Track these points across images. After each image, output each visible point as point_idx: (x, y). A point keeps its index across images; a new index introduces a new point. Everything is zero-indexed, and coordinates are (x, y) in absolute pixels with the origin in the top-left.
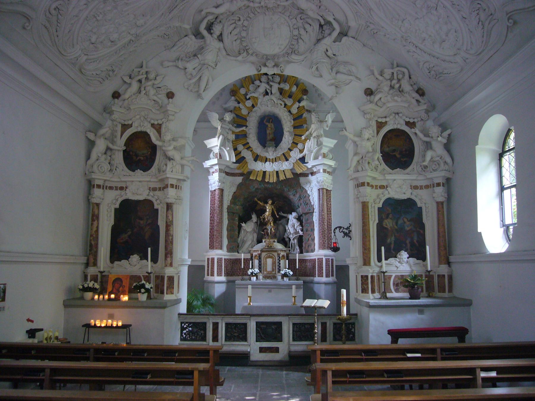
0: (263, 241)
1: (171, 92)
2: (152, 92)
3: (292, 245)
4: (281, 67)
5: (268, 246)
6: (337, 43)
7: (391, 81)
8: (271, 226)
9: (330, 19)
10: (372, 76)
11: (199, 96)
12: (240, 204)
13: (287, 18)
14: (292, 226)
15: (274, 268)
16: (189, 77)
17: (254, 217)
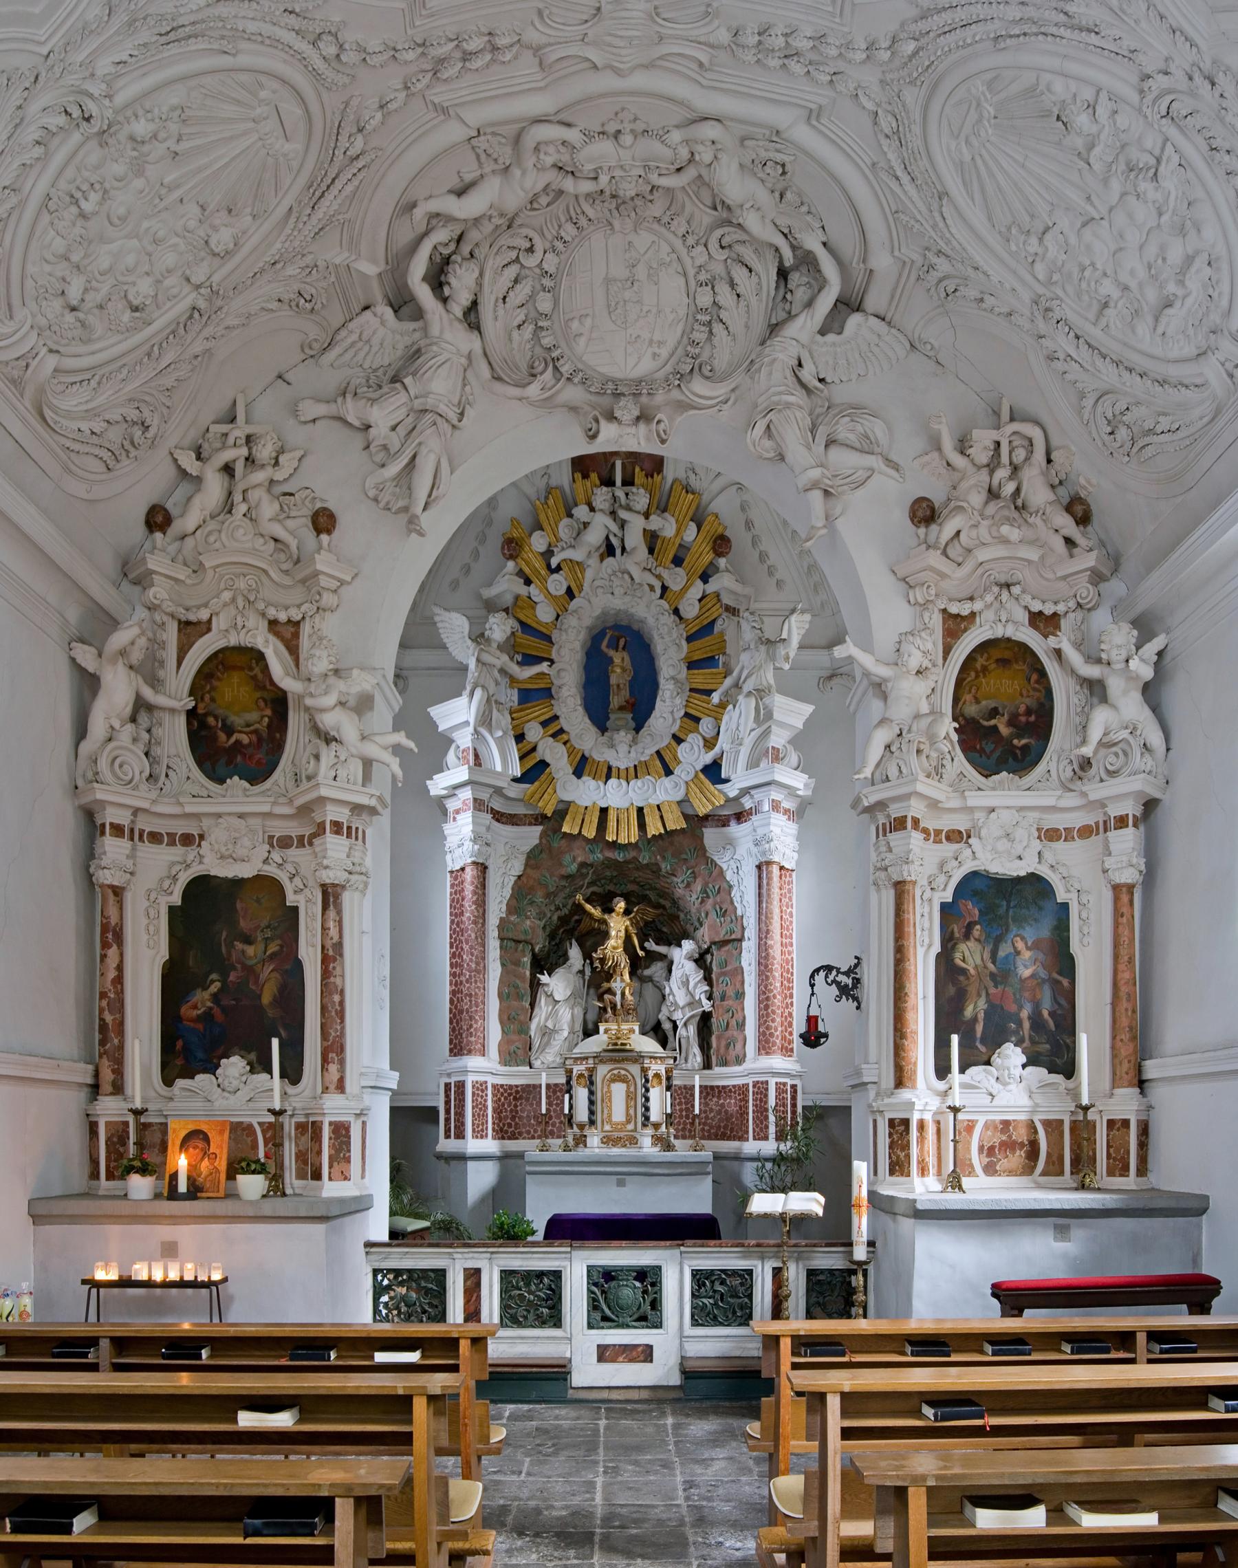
1: (325, 509)
2: (268, 509)
4: (659, 422)
6: (831, 337)
7: (992, 472)
9: (812, 243)
10: (936, 454)
11: (413, 525)
13: (678, 243)
16: (380, 457)
17: (575, 953)
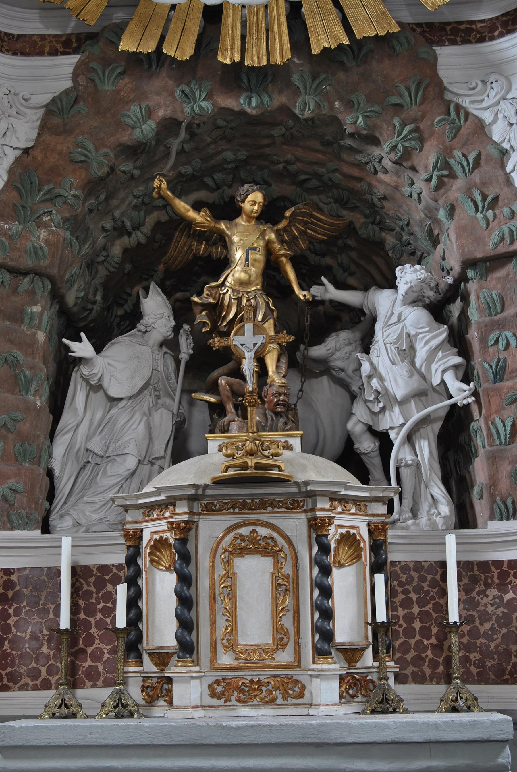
0: (213, 445)
3: (403, 470)
5: (245, 466)
8: (258, 330)
12: (58, 218)
14: (400, 351)
15: (287, 622)
